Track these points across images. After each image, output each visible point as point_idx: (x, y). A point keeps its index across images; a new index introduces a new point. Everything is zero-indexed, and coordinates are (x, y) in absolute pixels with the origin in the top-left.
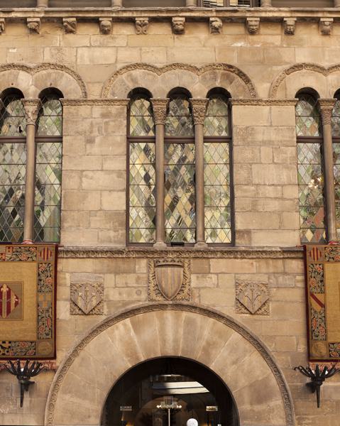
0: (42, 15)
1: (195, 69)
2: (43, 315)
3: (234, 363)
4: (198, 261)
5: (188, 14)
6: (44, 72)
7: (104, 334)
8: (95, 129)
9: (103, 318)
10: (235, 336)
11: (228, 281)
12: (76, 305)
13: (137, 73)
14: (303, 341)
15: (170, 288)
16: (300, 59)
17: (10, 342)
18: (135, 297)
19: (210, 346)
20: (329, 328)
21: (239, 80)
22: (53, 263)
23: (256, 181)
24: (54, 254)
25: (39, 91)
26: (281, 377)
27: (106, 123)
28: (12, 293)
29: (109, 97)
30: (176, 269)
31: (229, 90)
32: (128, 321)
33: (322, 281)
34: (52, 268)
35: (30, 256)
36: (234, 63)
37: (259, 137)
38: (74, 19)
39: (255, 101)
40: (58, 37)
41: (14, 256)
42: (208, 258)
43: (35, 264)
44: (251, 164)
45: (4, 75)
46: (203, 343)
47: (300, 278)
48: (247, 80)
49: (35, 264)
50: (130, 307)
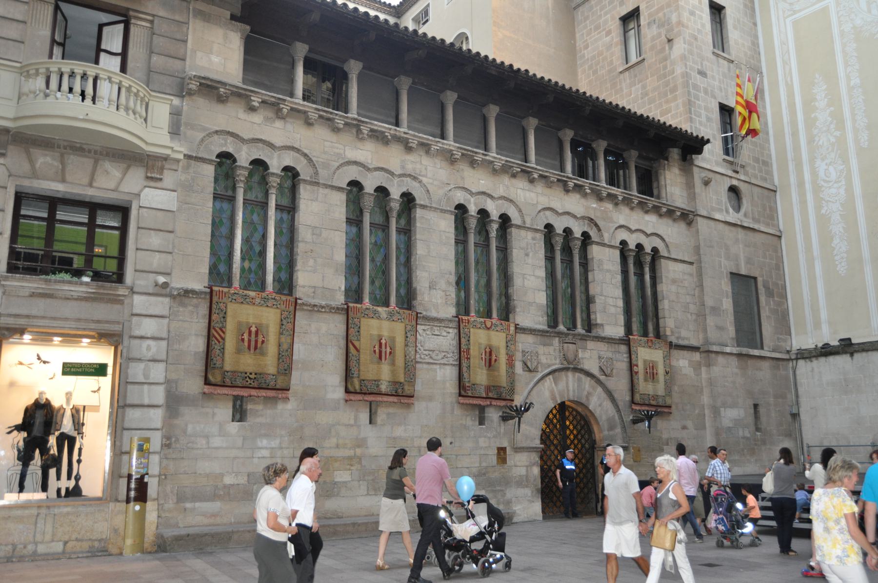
0: (503, 162)
1: (574, 217)
2: (283, 354)
3: (600, 405)
4: (582, 341)
5: (575, 181)
8: (529, 247)
9: (540, 375)
10: (599, 389)
11: (595, 355)
12: (526, 364)
13: (548, 213)
15: (571, 356)
16: (622, 222)
17: (256, 374)
18: (554, 362)
19: (589, 394)
20: (362, 368)
21: (594, 227)
22: (293, 312)
24: (293, 304)
26: (621, 415)
27: (535, 244)
28: (259, 333)
29: (535, 227)
30: (574, 345)
32: (551, 377)
33: (224, 317)
34: (292, 316)
35: (275, 303)
37: (605, 267)
38: (519, 170)
39: (603, 245)
40: (506, 179)
41: (262, 302)
43: (661, 351)
44: (602, 283)
46: (585, 393)
47: (627, 355)
48: (599, 230)
49: (278, 311)
50: (554, 367)
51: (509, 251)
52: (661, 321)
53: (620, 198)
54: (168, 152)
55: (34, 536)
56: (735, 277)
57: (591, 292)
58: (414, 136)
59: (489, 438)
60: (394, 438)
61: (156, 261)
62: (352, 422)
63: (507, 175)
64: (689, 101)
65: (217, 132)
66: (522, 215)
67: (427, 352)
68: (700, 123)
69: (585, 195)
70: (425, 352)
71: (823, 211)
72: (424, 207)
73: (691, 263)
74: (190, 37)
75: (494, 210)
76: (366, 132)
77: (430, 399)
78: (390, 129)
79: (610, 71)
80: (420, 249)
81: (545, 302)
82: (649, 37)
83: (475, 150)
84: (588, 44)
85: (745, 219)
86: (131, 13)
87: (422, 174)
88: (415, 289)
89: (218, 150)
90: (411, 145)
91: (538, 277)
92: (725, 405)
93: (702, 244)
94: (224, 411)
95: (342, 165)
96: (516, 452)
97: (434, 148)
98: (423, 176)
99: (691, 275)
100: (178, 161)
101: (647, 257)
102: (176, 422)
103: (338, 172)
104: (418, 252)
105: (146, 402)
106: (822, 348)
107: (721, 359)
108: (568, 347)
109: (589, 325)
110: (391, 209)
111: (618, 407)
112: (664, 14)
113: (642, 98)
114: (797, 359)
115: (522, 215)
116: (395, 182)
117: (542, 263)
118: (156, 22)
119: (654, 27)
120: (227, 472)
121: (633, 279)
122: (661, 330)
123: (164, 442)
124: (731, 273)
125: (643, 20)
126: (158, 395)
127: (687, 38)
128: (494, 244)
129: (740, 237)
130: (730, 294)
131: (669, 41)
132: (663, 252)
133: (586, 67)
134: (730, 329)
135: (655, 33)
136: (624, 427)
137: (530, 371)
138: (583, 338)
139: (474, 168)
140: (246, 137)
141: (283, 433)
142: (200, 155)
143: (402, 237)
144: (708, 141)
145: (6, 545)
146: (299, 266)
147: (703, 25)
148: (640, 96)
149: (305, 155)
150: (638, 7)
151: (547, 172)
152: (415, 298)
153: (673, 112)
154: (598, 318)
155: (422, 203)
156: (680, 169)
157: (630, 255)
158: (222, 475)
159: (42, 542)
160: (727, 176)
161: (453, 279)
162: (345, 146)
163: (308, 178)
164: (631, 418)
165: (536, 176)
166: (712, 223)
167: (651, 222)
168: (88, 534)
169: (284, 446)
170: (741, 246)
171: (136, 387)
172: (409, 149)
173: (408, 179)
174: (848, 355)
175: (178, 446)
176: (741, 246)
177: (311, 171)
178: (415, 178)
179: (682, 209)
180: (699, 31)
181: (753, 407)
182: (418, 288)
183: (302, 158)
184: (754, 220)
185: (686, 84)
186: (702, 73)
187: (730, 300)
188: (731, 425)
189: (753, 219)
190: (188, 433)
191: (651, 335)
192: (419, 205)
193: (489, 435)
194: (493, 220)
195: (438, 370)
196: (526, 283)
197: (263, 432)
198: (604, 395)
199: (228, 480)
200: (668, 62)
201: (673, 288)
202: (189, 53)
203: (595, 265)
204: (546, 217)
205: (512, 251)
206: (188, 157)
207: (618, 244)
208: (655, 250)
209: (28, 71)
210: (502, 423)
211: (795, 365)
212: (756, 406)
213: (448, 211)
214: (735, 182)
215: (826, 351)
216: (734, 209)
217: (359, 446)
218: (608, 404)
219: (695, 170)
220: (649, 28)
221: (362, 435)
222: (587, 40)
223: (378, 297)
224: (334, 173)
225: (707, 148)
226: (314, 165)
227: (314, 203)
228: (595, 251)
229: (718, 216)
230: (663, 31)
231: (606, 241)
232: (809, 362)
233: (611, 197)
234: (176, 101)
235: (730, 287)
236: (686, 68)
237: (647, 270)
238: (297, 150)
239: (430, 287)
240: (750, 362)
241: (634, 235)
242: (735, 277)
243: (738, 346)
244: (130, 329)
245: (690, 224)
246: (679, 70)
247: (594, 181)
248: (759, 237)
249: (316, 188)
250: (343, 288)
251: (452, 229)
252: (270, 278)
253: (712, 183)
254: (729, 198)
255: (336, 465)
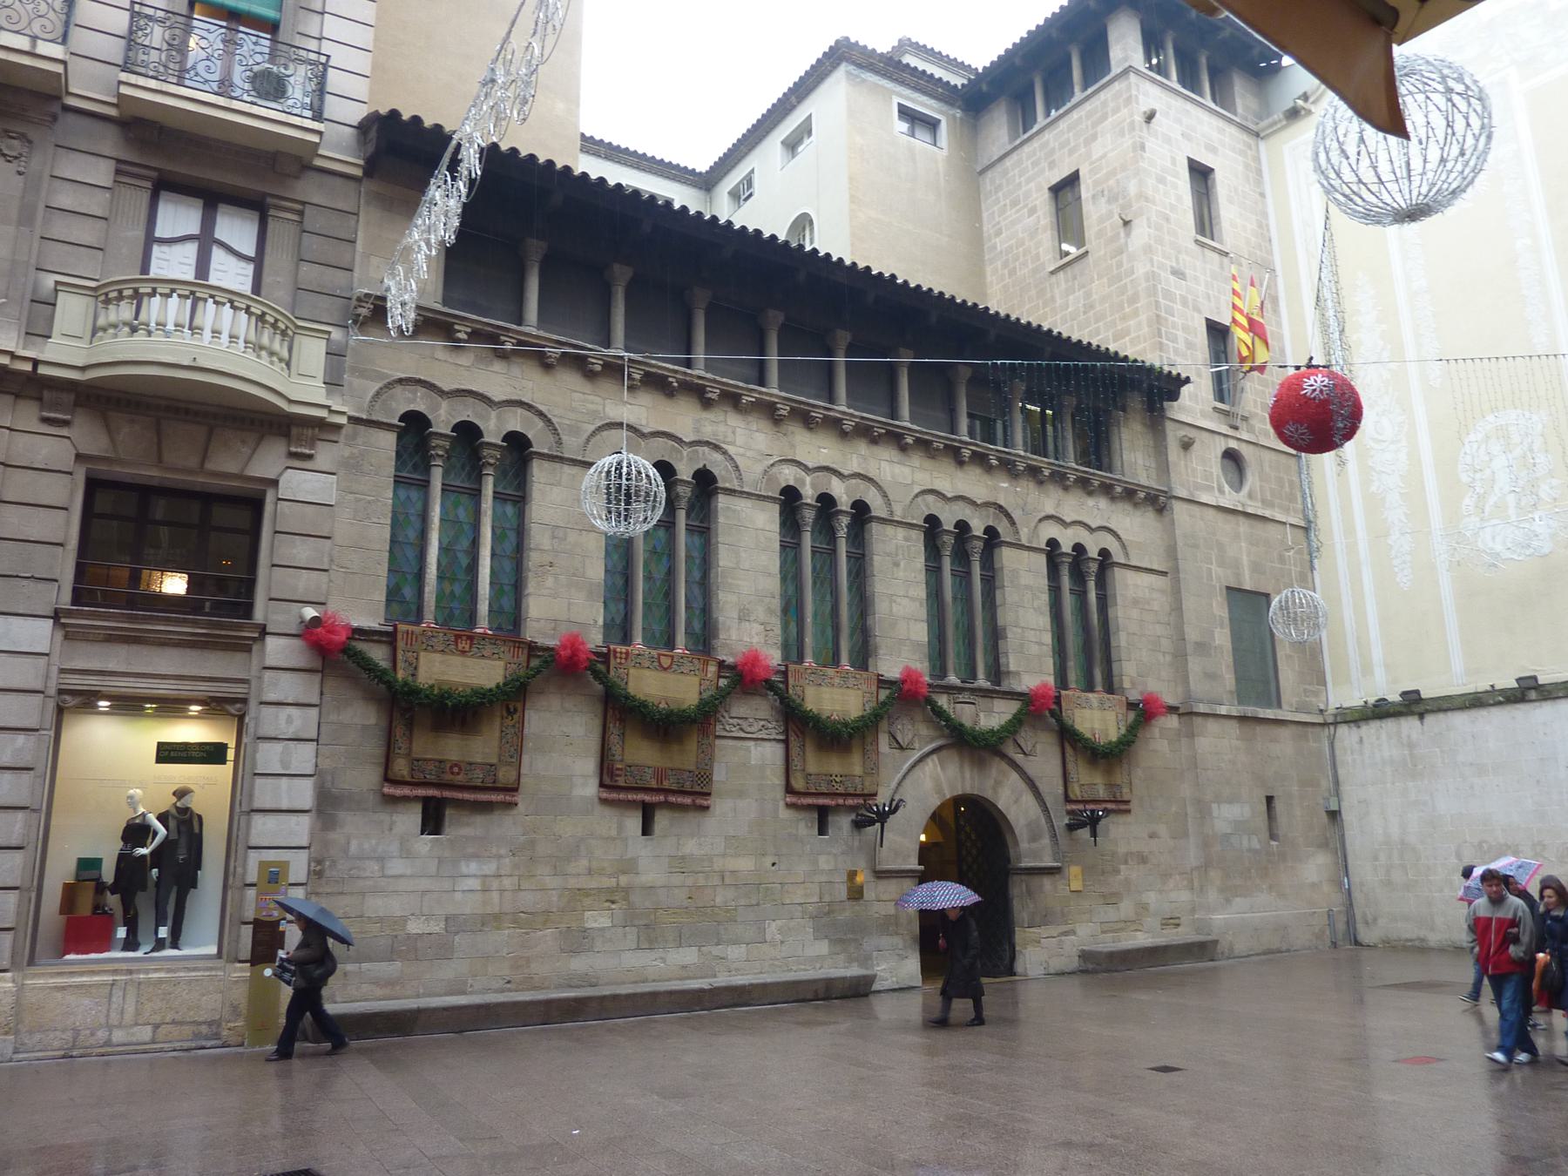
1: (973, 503)
3: (1016, 801)
6: (854, 481)
7: (917, 769)
8: (900, 552)
9: (917, 755)
12: (895, 738)
13: (930, 498)
14: (1061, 782)
16: (1050, 511)
23: (1022, 625)
25: (851, 502)
31: (1000, 530)
32: (935, 757)
36: (1002, 503)
37: (1023, 581)
38: (883, 431)
40: (862, 447)
42: (992, 697)
45: (818, 477)
48: (1013, 523)
51: (867, 558)
52: (1115, 666)
53: (1047, 473)
54: (323, 413)
55: (108, 1016)
56: (1234, 593)
57: (1000, 622)
58: (715, 381)
59: (835, 855)
60: (683, 858)
61: (303, 583)
62: (614, 833)
63: (863, 440)
64: (1158, 316)
65: (400, 381)
66: (888, 503)
67: (735, 721)
68: (1176, 351)
69: (989, 469)
70: (731, 721)
71: (1373, 489)
72: (731, 492)
73: (1164, 574)
74: (360, 234)
75: (842, 493)
76: (638, 377)
77: (741, 794)
78: (676, 372)
79: (1035, 271)
80: (724, 559)
81: (926, 639)
82: (1094, 217)
83: (811, 401)
84: (1000, 229)
85: (1249, 503)
86: (269, 200)
87: (729, 439)
88: (717, 621)
89: (403, 409)
90: (710, 395)
91: (912, 599)
92: (1219, 799)
93: (1180, 543)
94: (411, 819)
95: (600, 429)
96: (879, 878)
97: (745, 399)
98: (728, 443)
99: (1163, 591)
100: (338, 427)
101: (1091, 565)
102: (332, 835)
103: (593, 440)
104: (721, 563)
105: (284, 807)
106: (1375, 706)
107: (1212, 726)
108: (962, 709)
109: (997, 672)
110: (678, 496)
111: (1045, 804)
112: (1118, 182)
113: (1085, 313)
114: (1335, 724)
115: (888, 503)
116: (685, 453)
117: (922, 577)
118: (308, 210)
119: (1103, 200)
120: (413, 915)
121: (1068, 600)
122: (1116, 679)
123: (312, 868)
124: (1228, 588)
125: (1086, 189)
126: (303, 794)
127: (1154, 218)
128: (843, 547)
129: (1242, 529)
130: (1227, 621)
131: (1126, 223)
132: (1118, 556)
133: (999, 264)
134: (1227, 676)
135: (1104, 211)
136: (1054, 836)
137: (901, 748)
138: (986, 694)
139: (810, 429)
140: (446, 388)
141: (503, 851)
142: (374, 418)
143: (697, 540)
144: (1187, 380)
145: (63, 1031)
146: (531, 586)
147: (1179, 198)
148: (1082, 309)
149: (541, 414)
150: (1077, 171)
151: (927, 433)
152: (716, 636)
153: (1133, 335)
154: (1012, 662)
155: (727, 485)
156: (1145, 425)
157: (1063, 562)
158: (404, 919)
159: (120, 1026)
160: (1219, 434)
161: (776, 604)
162: (604, 399)
163: (546, 451)
164: (1067, 821)
165: (910, 440)
166: (1195, 509)
167: (1096, 510)
168: (192, 1013)
169: (503, 872)
170: (1243, 544)
171: (270, 780)
172: (707, 404)
173: (706, 449)
174: (1416, 717)
175: (334, 873)
176: (1243, 544)
177: (551, 438)
178: (716, 447)
179: (1147, 487)
180: (1173, 208)
181: (1264, 801)
182: (721, 619)
183: (536, 419)
184: (1266, 503)
185: (1152, 291)
186: (1178, 273)
187: (1227, 631)
188: (1229, 831)
189: (1263, 501)
190: (350, 854)
191: (1099, 688)
192: (722, 489)
193: (834, 851)
194: (841, 511)
195: (753, 748)
196: (895, 608)
197: (470, 850)
198: (1022, 785)
199: (414, 927)
200: (1124, 256)
201: (1135, 613)
202: (358, 258)
203: (1006, 579)
204: (927, 506)
205: (872, 559)
206: (354, 420)
207: (1043, 546)
208: (1104, 553)
209: (106, 294)
210: (856, 833)
211: (1332, 732)
212: (1270, 799)
213: (768, 497)
214: (1233, 444)
215: (1380, 711)
216: (1231, 487)
217: (624, 873)
218: (1028, 799)
219: (1169, 426)
220: (1094, 203)
221: (629, 856)
222: (999, 223)
223: (658, 635)
224: (588, 440)
225: (1185, 390)
226: (556, 430)
227: (555, 489)
228: (1008, 558)
229: (1205, 498)
230: (1116, 210)
231: (1024, 541)
232: (1355, 728)
233: (1033, 472)
234: (337, 334)
235: (1227, 611)
236: (1153, 266)
237: (1092, 585)
238: (528, 407)
239: (740, 619)
240: (1259, 729)
241: (1070, 531)
242: (1233, 592)
243: (1240, 703)
244: (260, 690)
245: (1161, 510)
246: (1141, 269)
247: (1006, 446)
248: (1272, 531)
249: (558, 465)
250: (601, 621)
251: (775, 526)
252: (483, 608)
253: (1195, 445)
254: (1223, 468)
255: (587, 902)
